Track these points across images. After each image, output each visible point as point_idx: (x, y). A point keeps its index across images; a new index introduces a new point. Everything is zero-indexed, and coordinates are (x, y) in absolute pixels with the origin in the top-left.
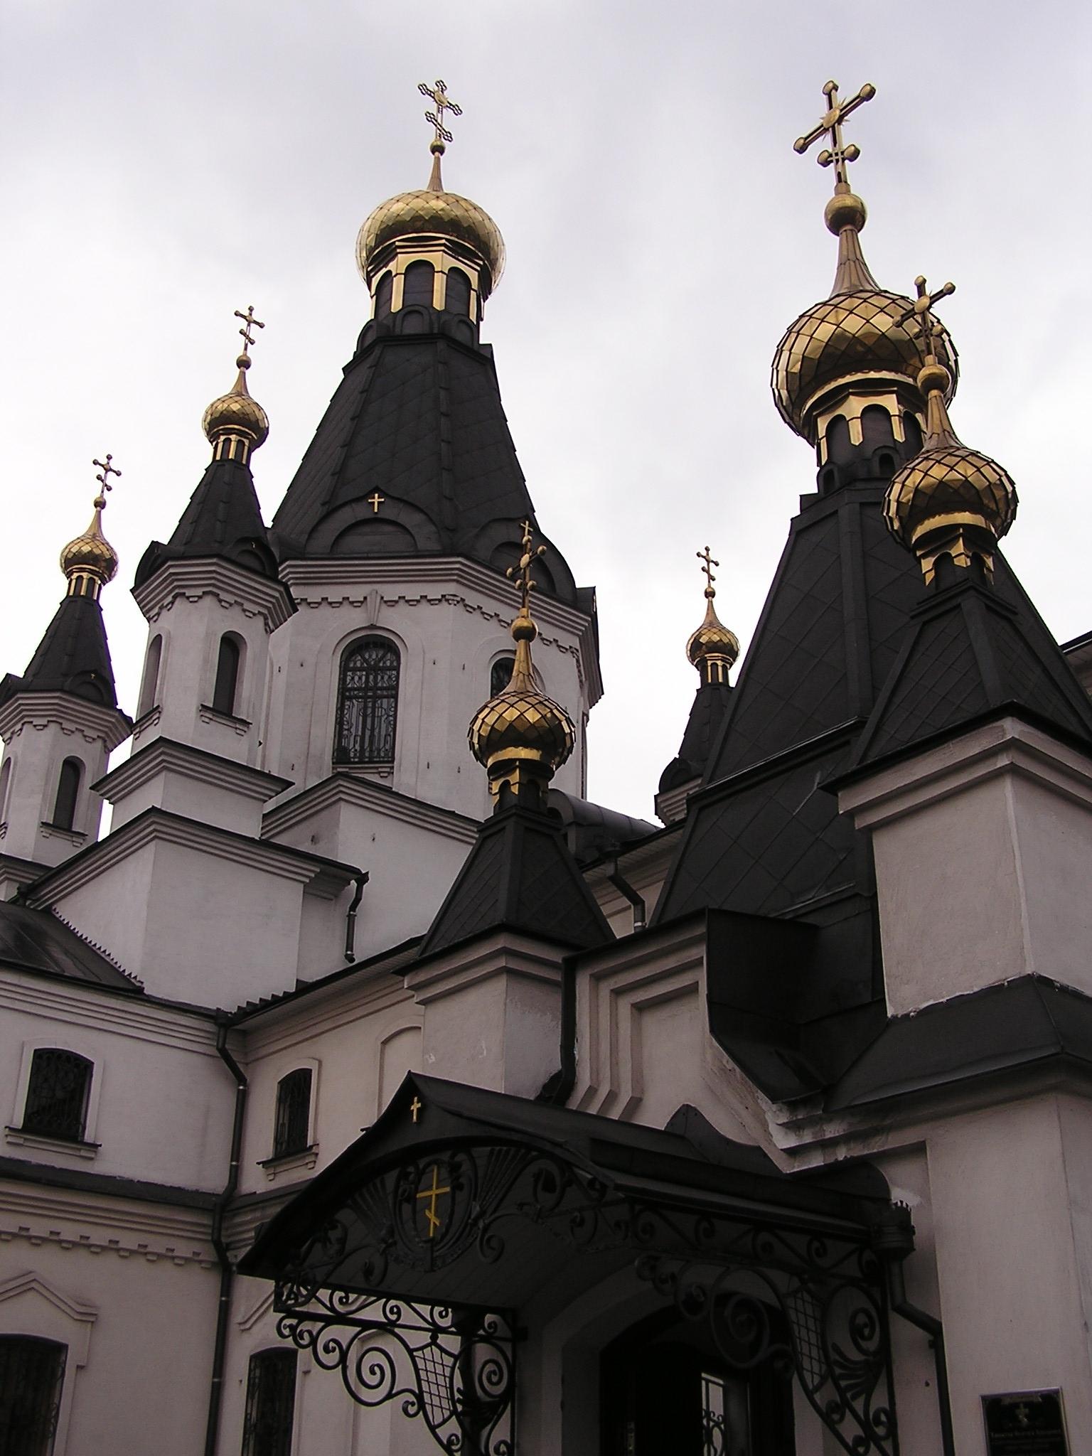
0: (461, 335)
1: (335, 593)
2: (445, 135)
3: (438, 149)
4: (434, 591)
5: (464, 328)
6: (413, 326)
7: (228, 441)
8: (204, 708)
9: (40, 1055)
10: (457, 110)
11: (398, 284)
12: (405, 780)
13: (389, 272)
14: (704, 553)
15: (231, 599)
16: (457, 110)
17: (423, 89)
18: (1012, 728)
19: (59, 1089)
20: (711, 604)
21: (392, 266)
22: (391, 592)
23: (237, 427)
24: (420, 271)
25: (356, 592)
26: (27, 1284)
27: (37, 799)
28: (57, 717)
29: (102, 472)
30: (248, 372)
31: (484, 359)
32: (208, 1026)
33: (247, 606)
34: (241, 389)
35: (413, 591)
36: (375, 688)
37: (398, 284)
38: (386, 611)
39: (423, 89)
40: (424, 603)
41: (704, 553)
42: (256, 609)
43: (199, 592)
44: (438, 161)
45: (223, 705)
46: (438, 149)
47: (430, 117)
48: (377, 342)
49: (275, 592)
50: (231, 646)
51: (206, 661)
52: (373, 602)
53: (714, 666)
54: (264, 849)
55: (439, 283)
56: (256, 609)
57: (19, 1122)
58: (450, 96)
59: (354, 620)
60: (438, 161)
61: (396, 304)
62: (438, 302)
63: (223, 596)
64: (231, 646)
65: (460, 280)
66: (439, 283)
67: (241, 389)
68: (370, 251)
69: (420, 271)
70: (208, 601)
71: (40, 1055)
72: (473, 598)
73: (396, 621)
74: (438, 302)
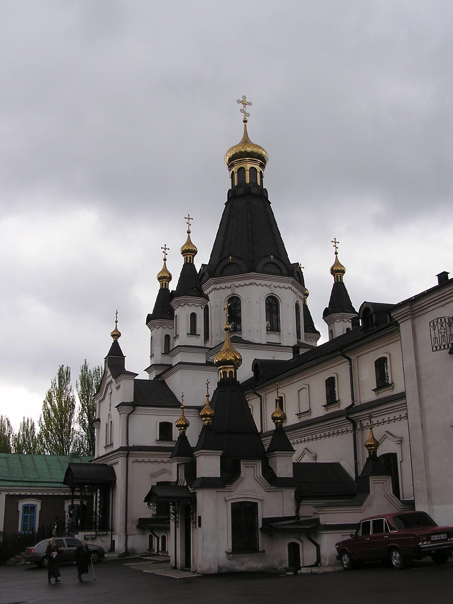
0: (254, 191)
1: (223, 285)
2: (247, 115)
3: (245, 121)
4: (247, 282)
5: (255, 187)
6: (241, 191)
7: (187, 257)
8: (188, 334)
9: (161, 424)
10: (250, 104)
11: (236, 175)
12: (245, 336)
13: (233, 171)
14: (334, 240)
15: (191, 304)
16: (250, 104)
17: (239, 102)
18: (202, 451)
19: (165, 429)
20: (337, 256)
21: (234, 169)
22: (237, 283)
23: (189, 252)
24: (241, 170)
25: (228, 285)
26: (164, 471)
27: (160, 347)
28: (161, 325)
29: (164, 250)
30: (190, 234)
31: (263, 195)
32: (197, 410)
33: (196, 304)
34: (189, 242)
35: (242, 283)
36: (236, 310)
37: (236, 175)
38: (236, 289)
39: (239, 102)
40: (245, 286)
41: (334, 240)
42: (198, 305)
43: (183, 304)
44: (245, 125)
45: (193, 332)
46: (245, 121)
47: (242, 111)
48: (233, 195)
49: (202, 299)
50: (193, 316)
51: (188, 322)
52: (233, 287)
53: (337, 277)
54: (209, 364)
55: (247, 174)
56: (198, 305)
57: (158, 439)
58: (248, 100)
59: (228, 293)
60: (245, 125)
61: (236, 184)
62: (248, 181)
63: (189, 304)
64: (193, 316)
65: (253, 169)
66: (247, 174)
67: (189, 242)
68: (228, 165)
69: (241, 170)
70: (186, 305)
71: (161, 424)
72: (258, 282)
73: (239, 292)
74: (248, 181)
